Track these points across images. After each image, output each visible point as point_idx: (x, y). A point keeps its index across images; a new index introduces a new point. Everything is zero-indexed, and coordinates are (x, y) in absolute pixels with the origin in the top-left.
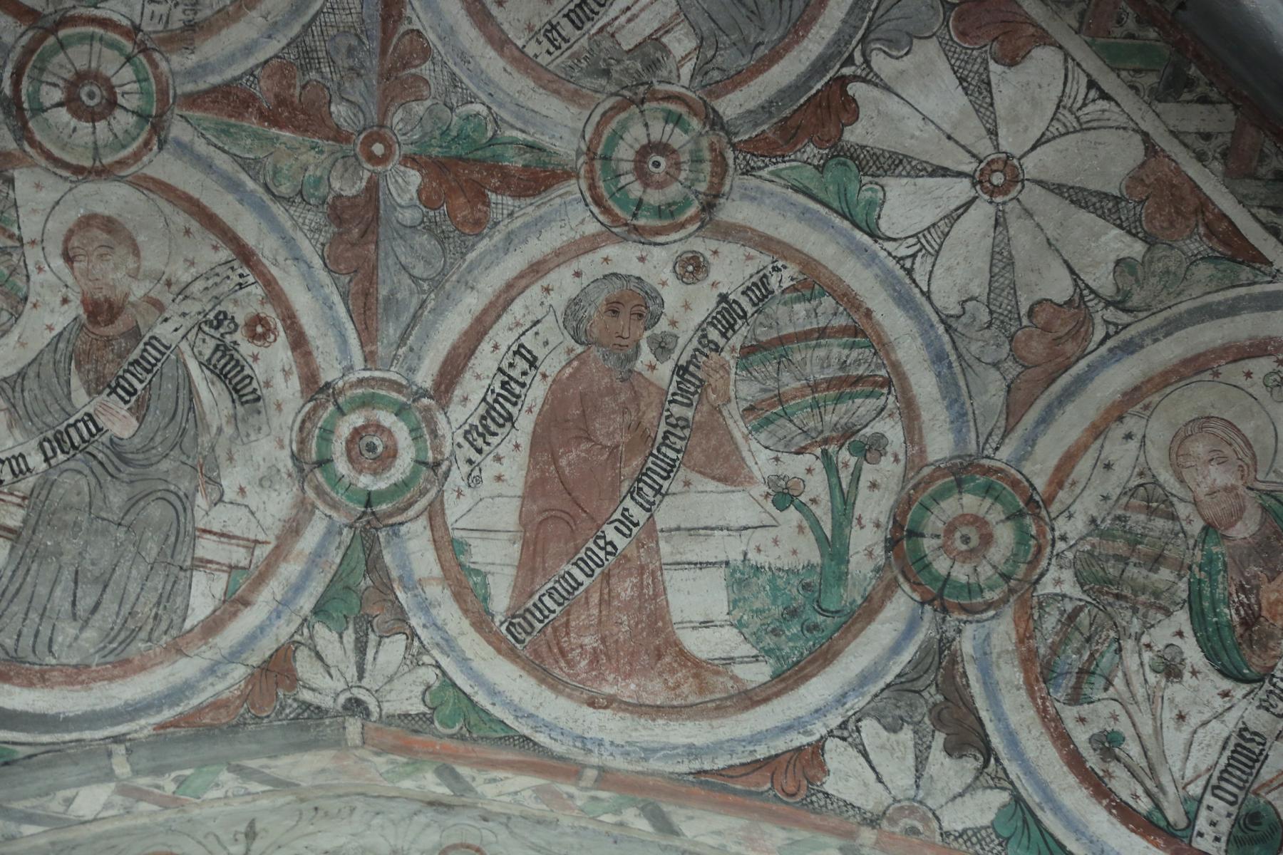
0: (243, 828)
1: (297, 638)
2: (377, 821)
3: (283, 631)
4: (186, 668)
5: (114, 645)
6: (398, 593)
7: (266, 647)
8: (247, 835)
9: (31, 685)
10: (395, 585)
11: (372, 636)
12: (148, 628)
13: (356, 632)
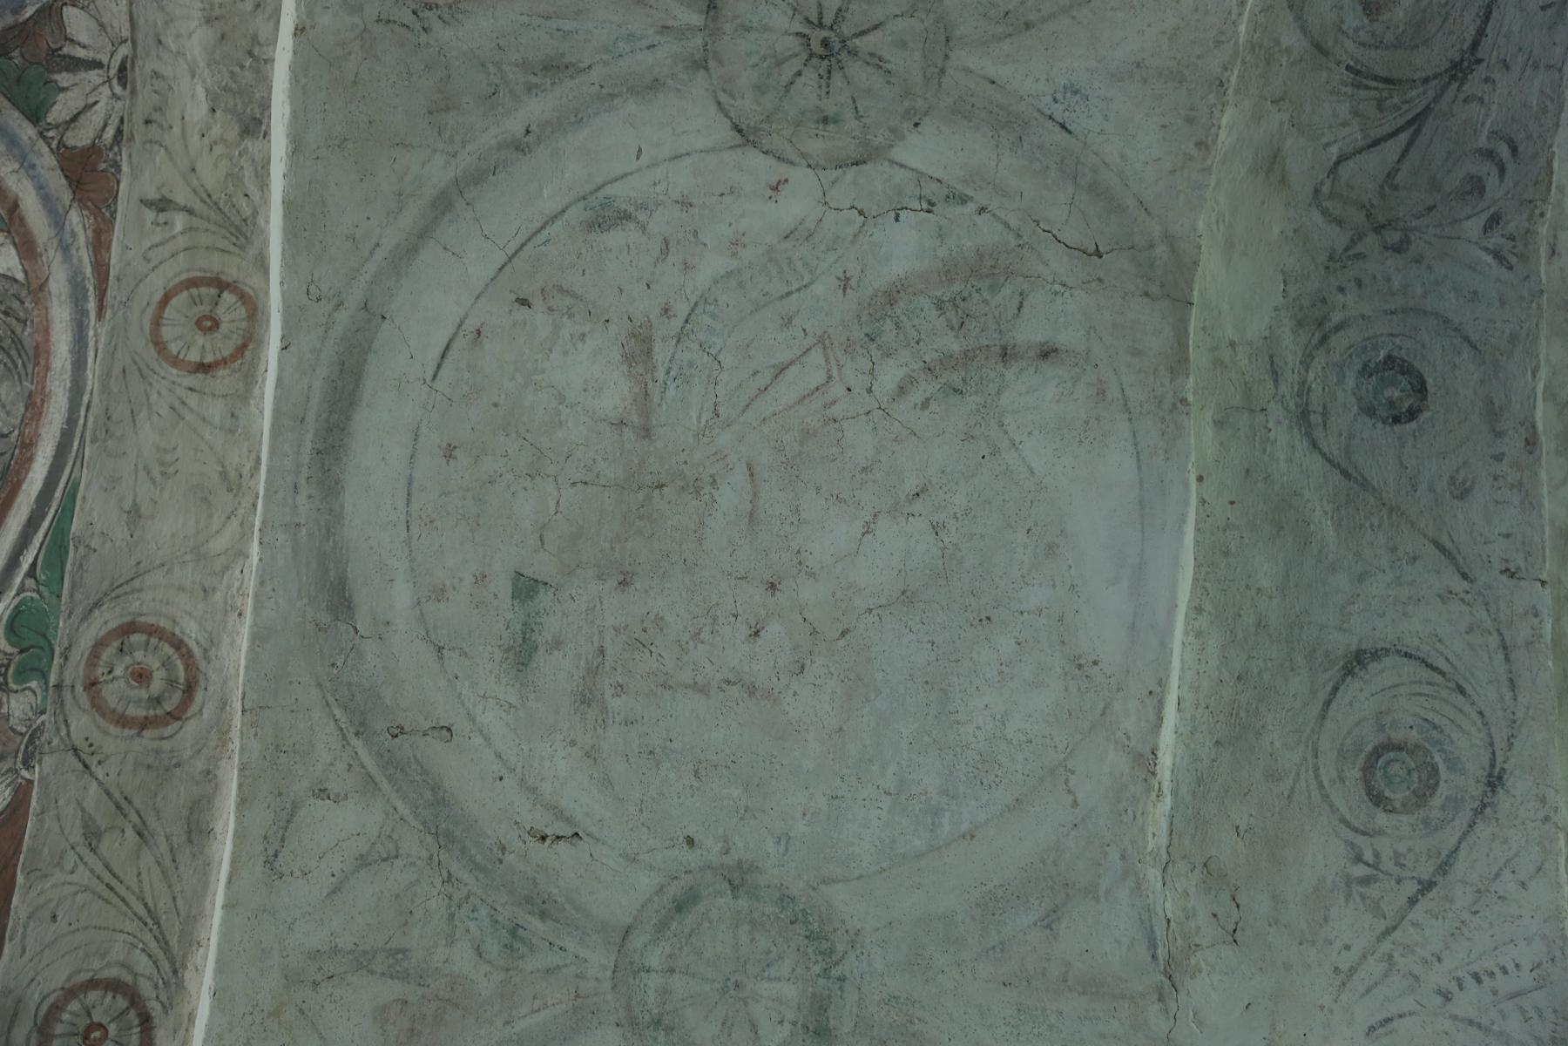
0: (150, 215)
1: (54, 144)
2: (169, 41)
3: (47, 160)
4: (58, 283)
5: (20, 363)
6: (27, 15)
7: (57, 183)
8: (162, 210)
9: (30, 460)
10: (22, 19)
11: (66, 50)
12: (14, 322)
13: (60, 72)
